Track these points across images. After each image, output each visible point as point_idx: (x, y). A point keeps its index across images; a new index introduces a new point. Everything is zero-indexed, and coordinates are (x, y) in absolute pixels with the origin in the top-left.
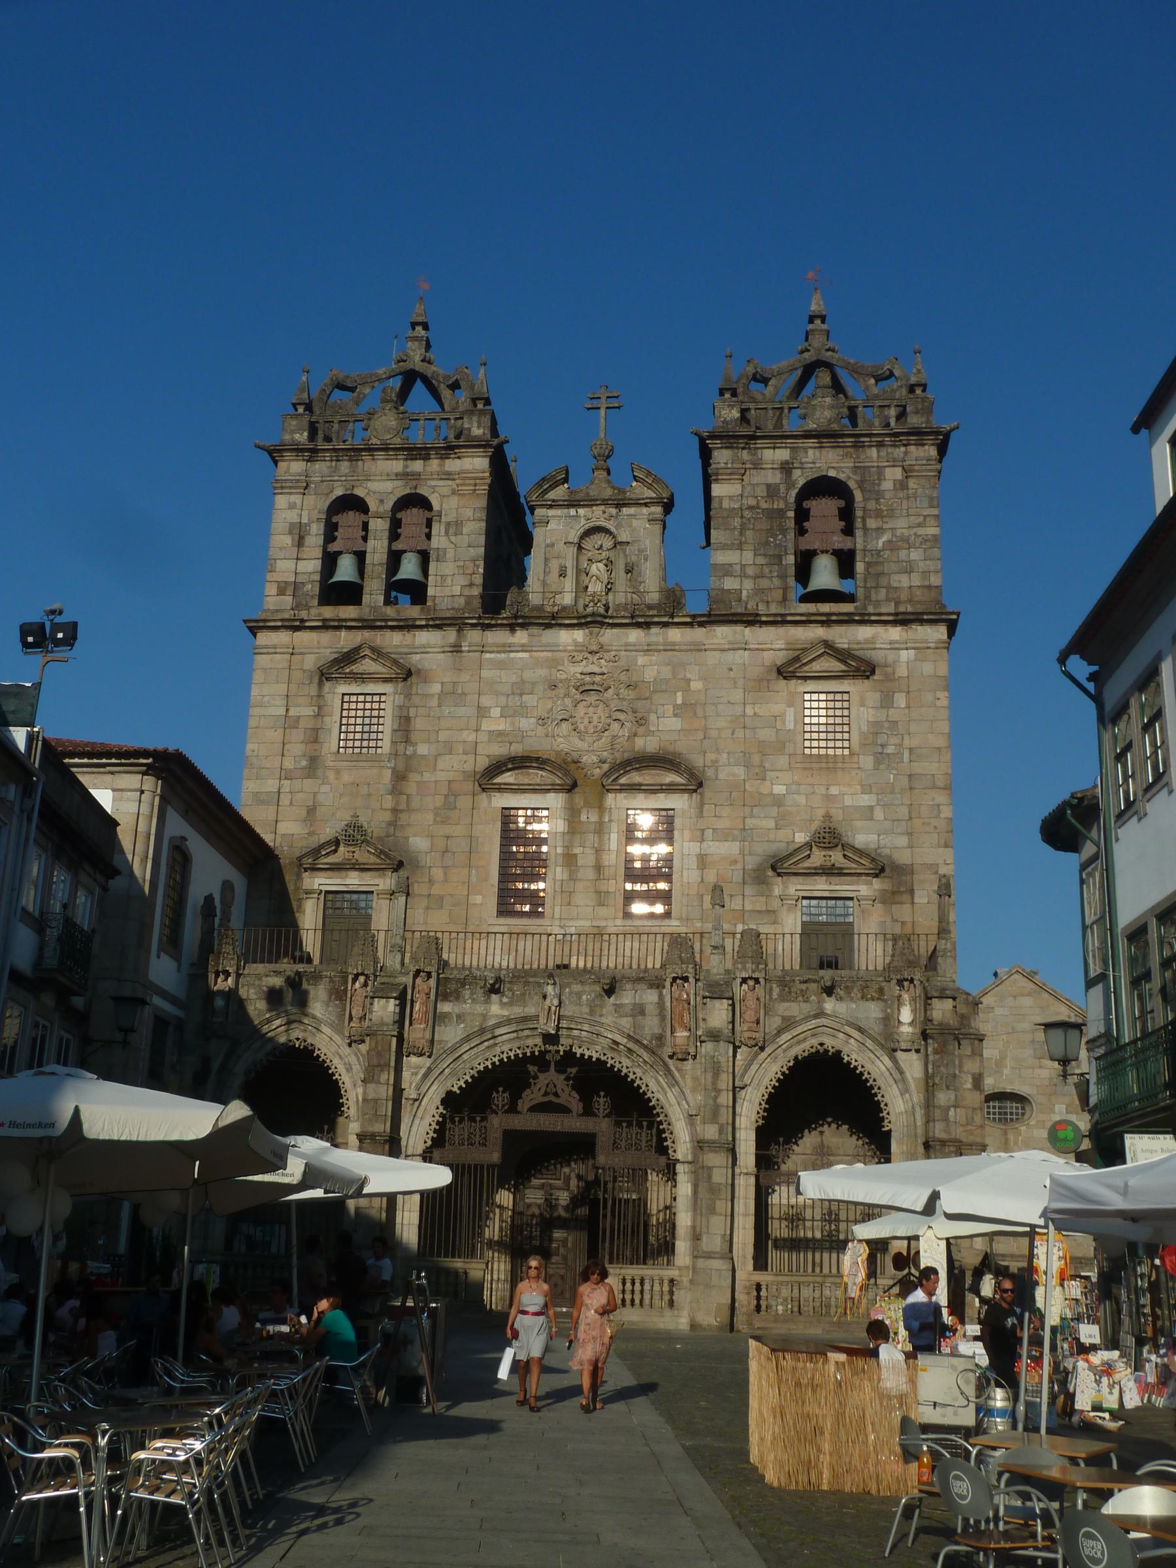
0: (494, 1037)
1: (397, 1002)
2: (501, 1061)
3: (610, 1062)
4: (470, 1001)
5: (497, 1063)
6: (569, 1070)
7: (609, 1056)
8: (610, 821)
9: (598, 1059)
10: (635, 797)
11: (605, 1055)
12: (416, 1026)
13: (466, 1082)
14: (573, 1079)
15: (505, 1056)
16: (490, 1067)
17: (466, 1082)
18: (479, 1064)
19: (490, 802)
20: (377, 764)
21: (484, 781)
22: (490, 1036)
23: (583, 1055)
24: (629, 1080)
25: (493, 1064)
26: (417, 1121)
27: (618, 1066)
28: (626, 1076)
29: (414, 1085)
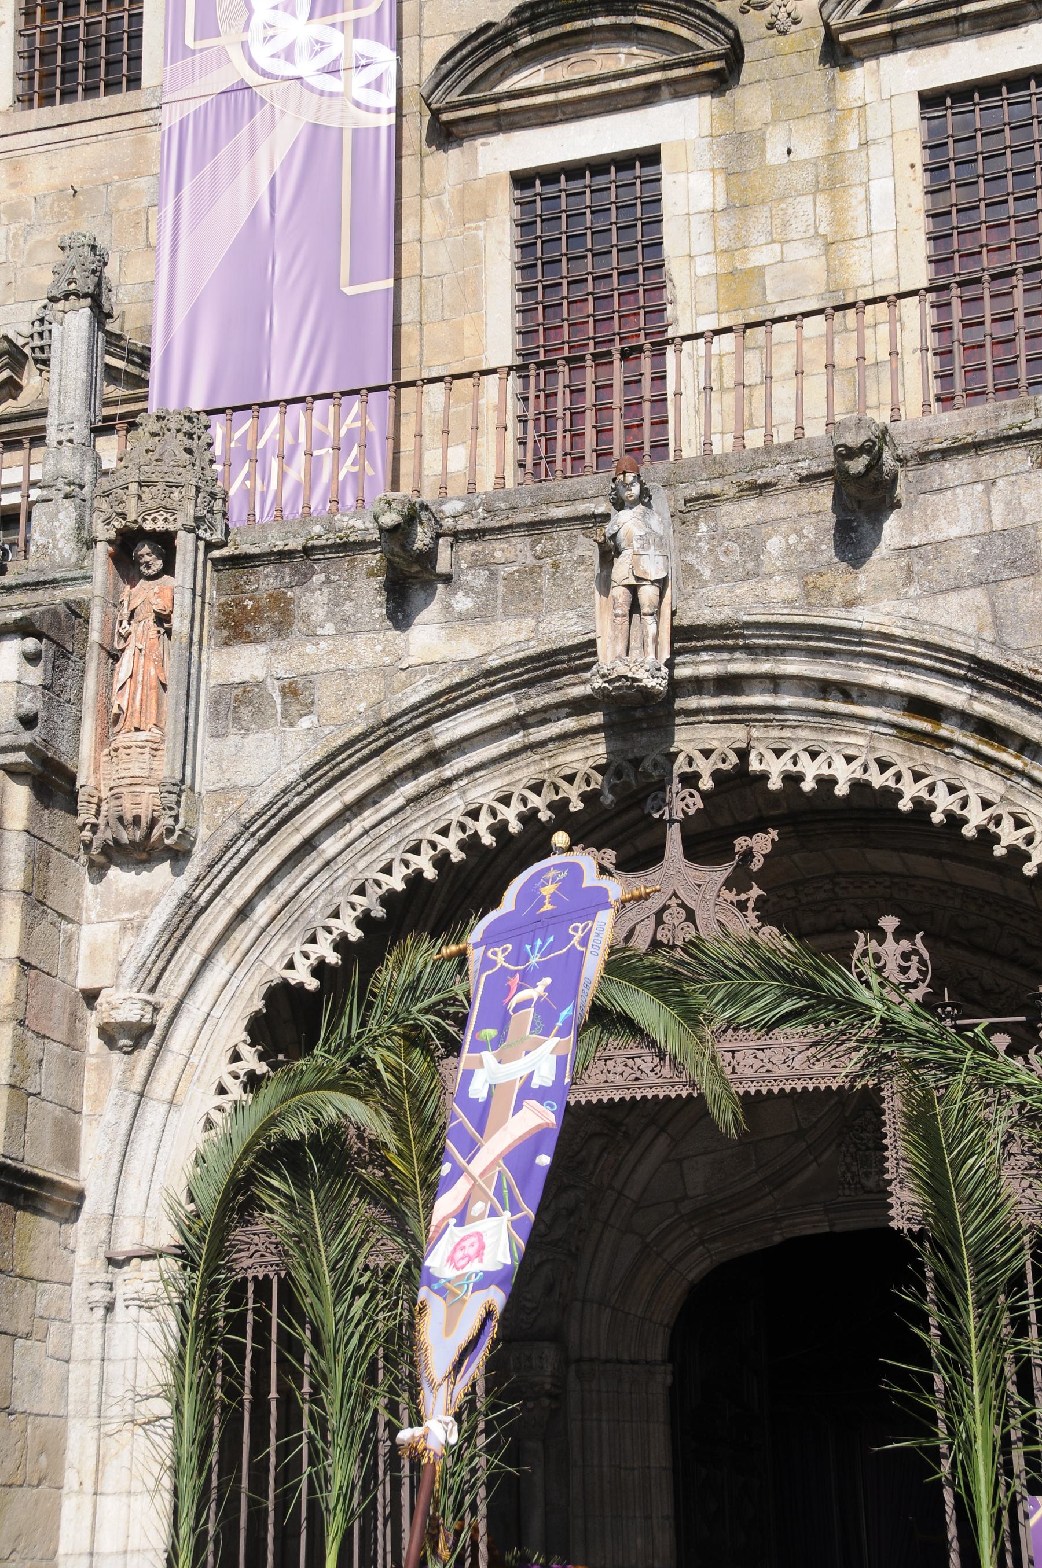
0: (436, 758)
1: (31, 644)
2: (472, 844)
3: (910, 791)
4: (330, 628)
5: (457, 856)
6: (741, 843)
7: (903, 766)
8: (865, 144)
9: (859, 786)
10: (946, 54)
11: (884, 766)
12: (123, 739)
13: (342, 945)
14: (760, 878)
15: (482, 826)
16: (430, 873)
17: (342, 945)
18: (388, 870)
19: (474, 162)
20: (127, 121)
21: (454, 97)
22: (417, 752)
23: (793, 779)
24: (999, 851)
25: (442, 861)
26: (154, 1113)
27: (944, 802)
28: (987, 837)
29: (130, 970)
